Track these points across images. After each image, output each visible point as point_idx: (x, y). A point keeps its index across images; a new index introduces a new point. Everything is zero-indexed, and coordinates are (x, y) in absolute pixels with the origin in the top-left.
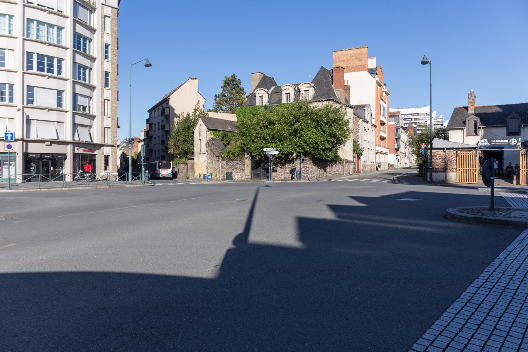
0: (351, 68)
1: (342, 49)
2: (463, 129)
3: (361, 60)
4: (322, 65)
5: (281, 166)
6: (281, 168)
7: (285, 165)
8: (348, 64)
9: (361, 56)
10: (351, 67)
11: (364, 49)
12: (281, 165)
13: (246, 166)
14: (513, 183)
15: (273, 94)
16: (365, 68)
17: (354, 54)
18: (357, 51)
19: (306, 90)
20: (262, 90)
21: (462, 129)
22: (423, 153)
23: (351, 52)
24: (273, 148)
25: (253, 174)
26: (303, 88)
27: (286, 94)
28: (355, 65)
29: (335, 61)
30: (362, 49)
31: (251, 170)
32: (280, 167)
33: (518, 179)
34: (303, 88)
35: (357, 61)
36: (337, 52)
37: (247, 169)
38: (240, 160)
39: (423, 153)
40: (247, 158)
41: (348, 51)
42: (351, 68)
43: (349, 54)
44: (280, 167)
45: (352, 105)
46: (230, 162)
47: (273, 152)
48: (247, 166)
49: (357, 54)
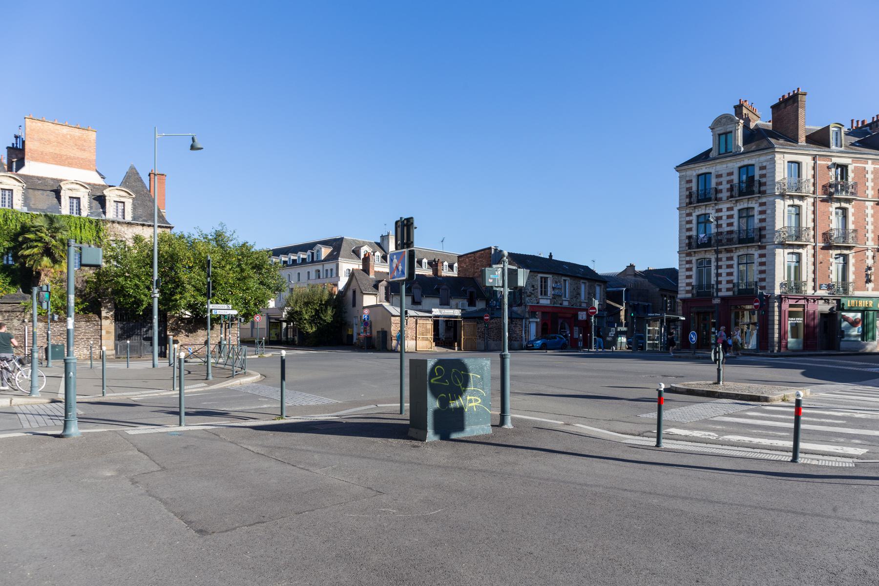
0: (63, 159)
1: (90, 128)
2: (376, 294)
3: (84, 150)
4: (132, 164)
5: (187, 334)
6: (188, 336)
7: (195, 332)
8: (57, 149)
9: (84, 144)
10: (65, 157)
11: (90, 133)
12: (186, 331)
13: (104, 333)
14: (455, 350)
15: (30, 191)
16: (92, 166)
17: (71, 135)
18: (77, 133)
19: (119, 200)
20: (10, 177)
21: (376, 295)
22: (366, 319)
23: (65, 130)
24: (226, 305)
25: (120, 346)
26: (113, 195)
27: (70, 197)
28: (72, 155)
29: (31, 136)
30: (87, 132)
31: (115, 340)
32: (186, 335)
33: (459, 345)
34: (111, 195)
35: (77, 150)
36: (34, 121)
37: (108, 339)
38: (86, 321)
39: (366, 319)
40: (107, 318)
41: (58, 127)
42: (63, 159)
43: (60, 132)
44: (186, 335)
45: (257, 248)
46: (58, 323)
47: (226, 311)
48: (108, 332)
49: (76, 138)
